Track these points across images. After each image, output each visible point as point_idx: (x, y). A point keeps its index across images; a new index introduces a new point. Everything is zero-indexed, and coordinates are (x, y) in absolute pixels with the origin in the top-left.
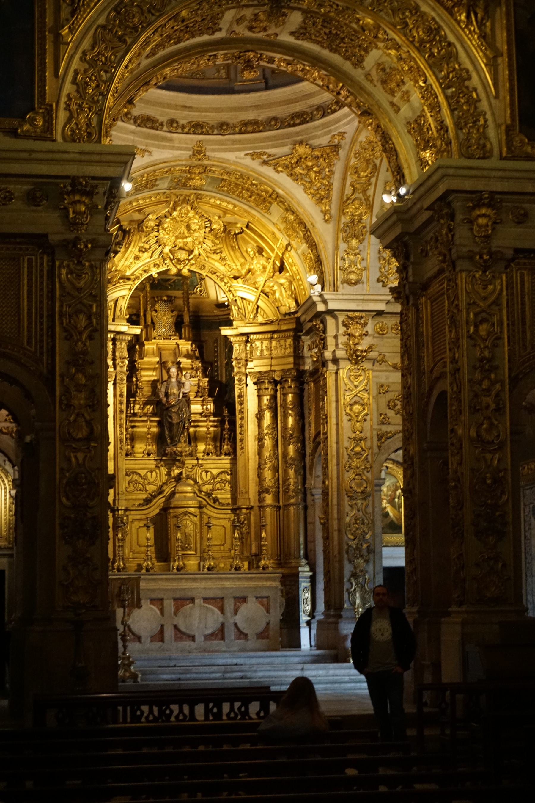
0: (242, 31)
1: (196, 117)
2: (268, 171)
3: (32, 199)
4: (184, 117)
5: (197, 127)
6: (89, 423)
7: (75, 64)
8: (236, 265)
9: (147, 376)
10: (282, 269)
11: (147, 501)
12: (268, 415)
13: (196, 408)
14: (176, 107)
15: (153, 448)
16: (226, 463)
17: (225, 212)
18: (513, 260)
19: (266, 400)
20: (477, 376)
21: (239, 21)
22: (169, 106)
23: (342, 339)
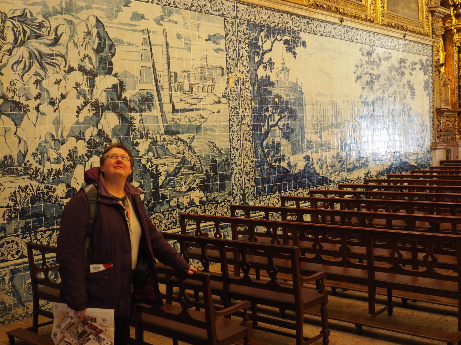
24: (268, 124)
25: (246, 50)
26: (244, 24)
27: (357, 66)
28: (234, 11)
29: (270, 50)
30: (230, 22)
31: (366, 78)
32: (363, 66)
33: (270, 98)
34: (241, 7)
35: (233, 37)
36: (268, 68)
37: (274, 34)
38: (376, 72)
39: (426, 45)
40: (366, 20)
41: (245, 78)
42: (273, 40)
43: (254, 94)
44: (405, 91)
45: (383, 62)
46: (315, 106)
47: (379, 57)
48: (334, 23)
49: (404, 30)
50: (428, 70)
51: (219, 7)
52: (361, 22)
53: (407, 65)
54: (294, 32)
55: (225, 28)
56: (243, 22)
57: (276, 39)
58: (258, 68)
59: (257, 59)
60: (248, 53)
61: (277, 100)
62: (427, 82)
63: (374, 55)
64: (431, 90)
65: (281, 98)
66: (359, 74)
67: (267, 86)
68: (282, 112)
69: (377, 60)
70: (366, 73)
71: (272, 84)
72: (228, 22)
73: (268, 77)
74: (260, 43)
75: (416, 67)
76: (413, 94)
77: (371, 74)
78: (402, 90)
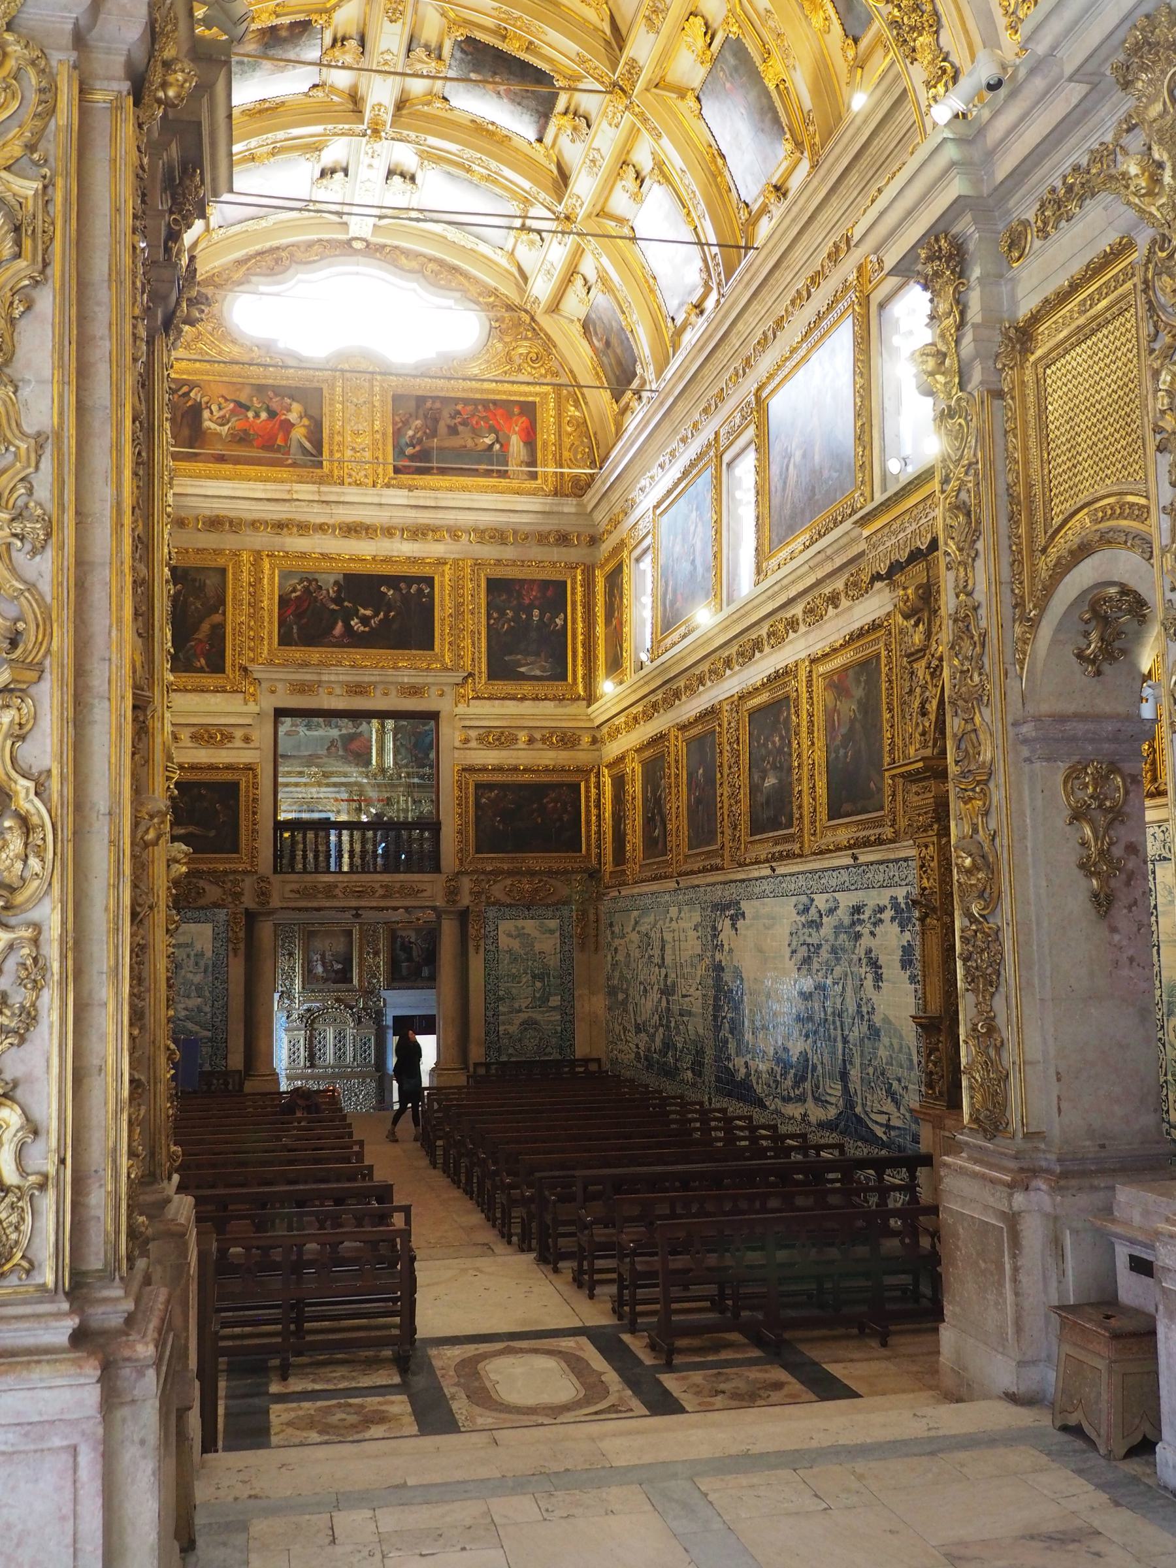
31: (803, 952)
32: (800, 933)
38: (814, 940)
39: (906, 860)
44: (863, 971)
50: (909, 919)
53: (865, 917)
62: (907, 950)
63: (813, 911)
64: (918, 965)
66: (794, 946)
75: (882, 916)
76: (878, 978)
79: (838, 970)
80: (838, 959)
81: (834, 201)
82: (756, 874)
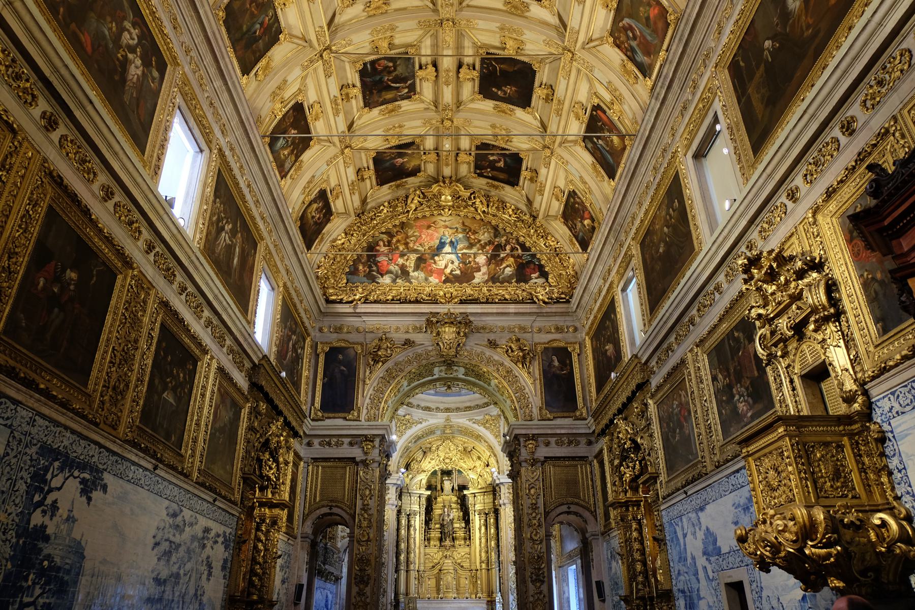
0: (443, 375)
1: (447, 406)
2: (475, 426)
3: (351, 444)
4: (442, 406)
5: (447, 410)
6: (368, 534)
7: (371, 392)
8: (470, 464)
9: (437, 512)
10: (488, 465)
11: (433, 567)
12: (483, 528)
13: (456, 525)
14: (438, 402)
15: (438, 543)
16: (467, 550)
17: (465, 443)
18: (545, 461)
19: (482, 521)
20: (530, 511)
21: (441, 371)
22: (435, 402)
23: (507, 495)
24: (21, 601)
25: (26, 483)
26: (36, 445)
27: (158, 528)
28: (29, 424)
29: (59, 489)
30: (18, 438)
31: (165, 546)
32: (166, 531)
33: (37, 559)
34: (40, 421)
35: (14, 461)
36: (49, 513)
37: (71, 468)
38: (177, 539)
39: (233, 515)
40: (181, 473)
41: (10, 522)
42: (67, 475)
43: (15, 550)
44: (203, 568)
45: (187, 529)
46: (95, 578)
47: (184, 521)
48: (146, 469)
49: (216, 493)
51: (9, 414)
52: (176, 474)
53: (210, 536)
54: (98, 471)
55: (8, 445)
56: (35, 441)
57: (72, 475)
58: (34, 511)
59: (37, 498)
60: (28, 487)
61: (46, 563)
62: (225, 561)
63: (179, 518)
64: (228, 570)
65: (53, 561)
66: (158, 539)
67: (38, 541)
68: (46, 584)
69: (181, 524)
70: (166, 540)
71: (47, 539)
72: (14, 437)
73: (44, 527)
74: (49, 476)
76: (210, 574)
77: (171, 542)
78: (199, 567)
79: (188, 566)
80: (190, 559)
81: (270, 198)
82: (134, 458)
